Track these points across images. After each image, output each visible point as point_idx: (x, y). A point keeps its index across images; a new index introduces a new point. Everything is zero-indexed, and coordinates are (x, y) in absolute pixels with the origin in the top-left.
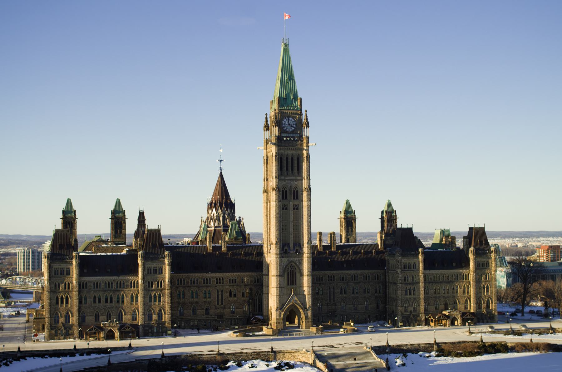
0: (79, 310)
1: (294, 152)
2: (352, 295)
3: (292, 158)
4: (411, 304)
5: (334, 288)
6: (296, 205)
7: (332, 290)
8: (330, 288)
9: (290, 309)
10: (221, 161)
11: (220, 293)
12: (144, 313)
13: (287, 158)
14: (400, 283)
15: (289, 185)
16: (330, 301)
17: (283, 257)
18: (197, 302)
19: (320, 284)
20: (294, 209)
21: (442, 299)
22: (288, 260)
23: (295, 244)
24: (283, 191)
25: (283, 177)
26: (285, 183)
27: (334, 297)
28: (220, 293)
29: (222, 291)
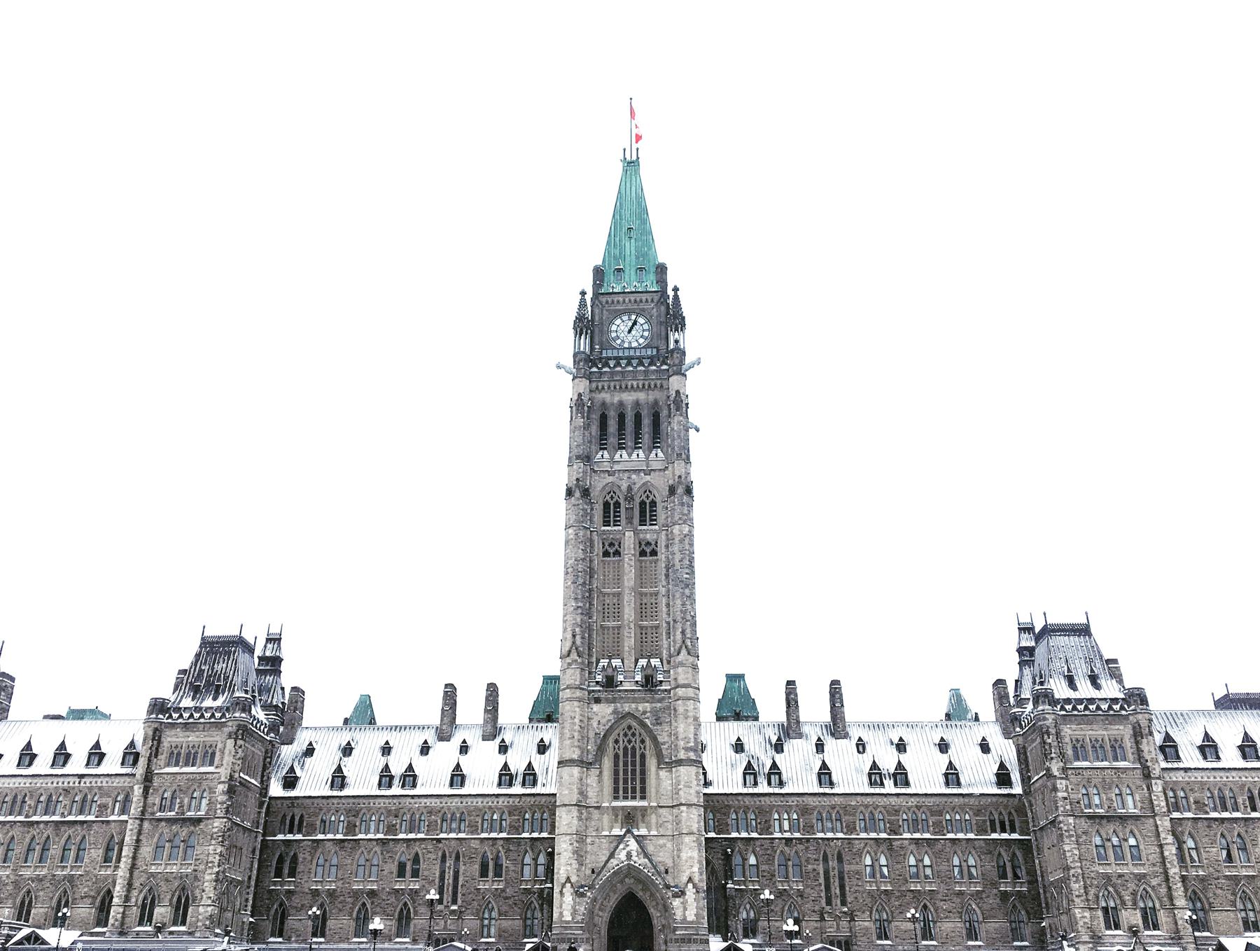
1: (641, 396)
3: (638, 417)
5: (840, 858)
6: (648, 544)
7: (833, 863)
8: (825, 859)
9: (621, 890)
11: (450, 862)
13: (622, 417)
15: (624, 486)
16: (829, 902)
17: (598, 701)
18: (372, 893)
19: (788, 840)
20: (643, 553)
22: (615, 712)
24: (606, 505)
26: (611, 479)
27: (842, 887)
28: (450, 862)
29: (457, 858)
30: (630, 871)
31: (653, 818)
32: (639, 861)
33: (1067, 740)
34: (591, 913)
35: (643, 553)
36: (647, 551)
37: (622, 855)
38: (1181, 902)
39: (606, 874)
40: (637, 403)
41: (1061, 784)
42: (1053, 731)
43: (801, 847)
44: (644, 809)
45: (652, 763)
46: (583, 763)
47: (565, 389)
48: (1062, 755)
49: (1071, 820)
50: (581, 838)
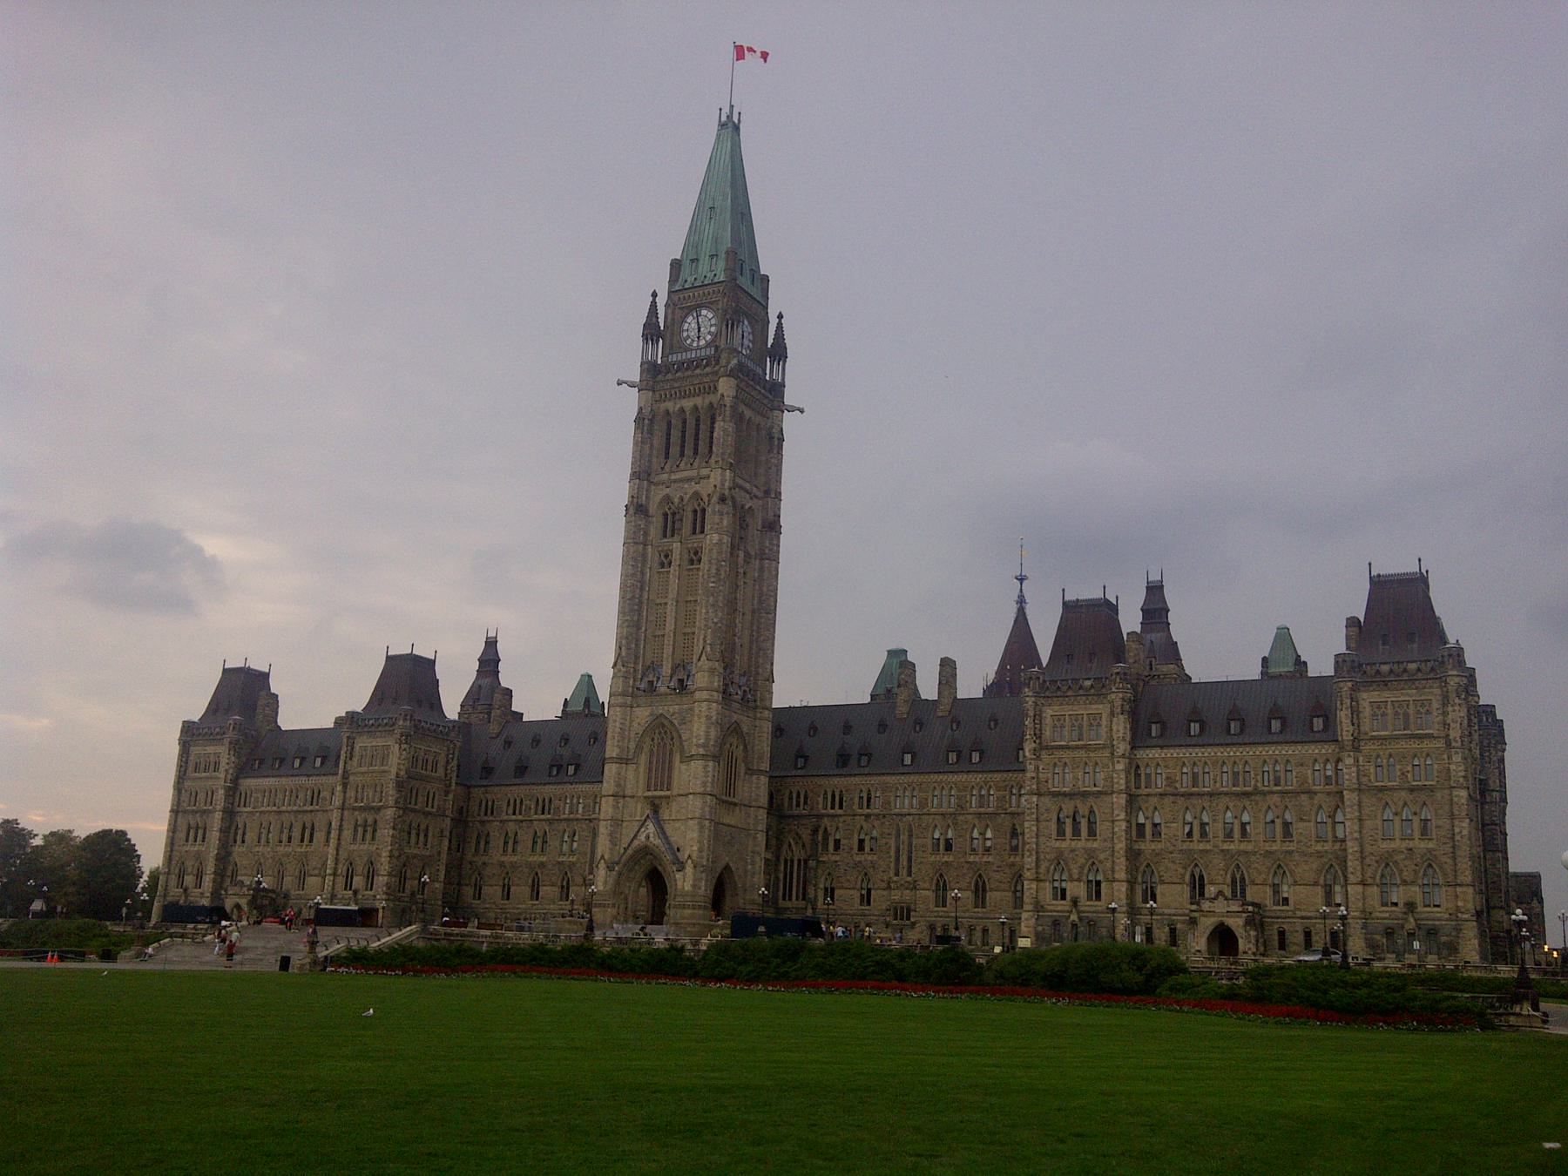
0: (223, 858)
1: (698, 401)
2: (972, 859)
4: (1075, 872)
7: (904, 837)
10: (1021, 579)
12: (335, 869)
14: (1031, 793)
16: (897, 874)
18: (542, 865)
19: (868, 816)
20: (692, 562)
21: (1219, 862)
23: (675, 669)
24: (666, 515)
25: (665, 476)
27: (910, 859)
30: (645, 851)
31: (674, 805)
32: (656, 841)
33: (1048, 720)
34: (617, 883)
35: (692, 562)
36: (695, 557)
37: (642, 837)
38: (1121, 875)
39: (630, 852)
40: (696, 408)
41: (1030, 767)
42: (1031, 713)
43: (876, 823)
44: (667, 797)
45: (677, 758)
46: (623, 760)
47: (630, 402)
48: (1038, 736)
49: (1035, 799)
50: (617, 823)
